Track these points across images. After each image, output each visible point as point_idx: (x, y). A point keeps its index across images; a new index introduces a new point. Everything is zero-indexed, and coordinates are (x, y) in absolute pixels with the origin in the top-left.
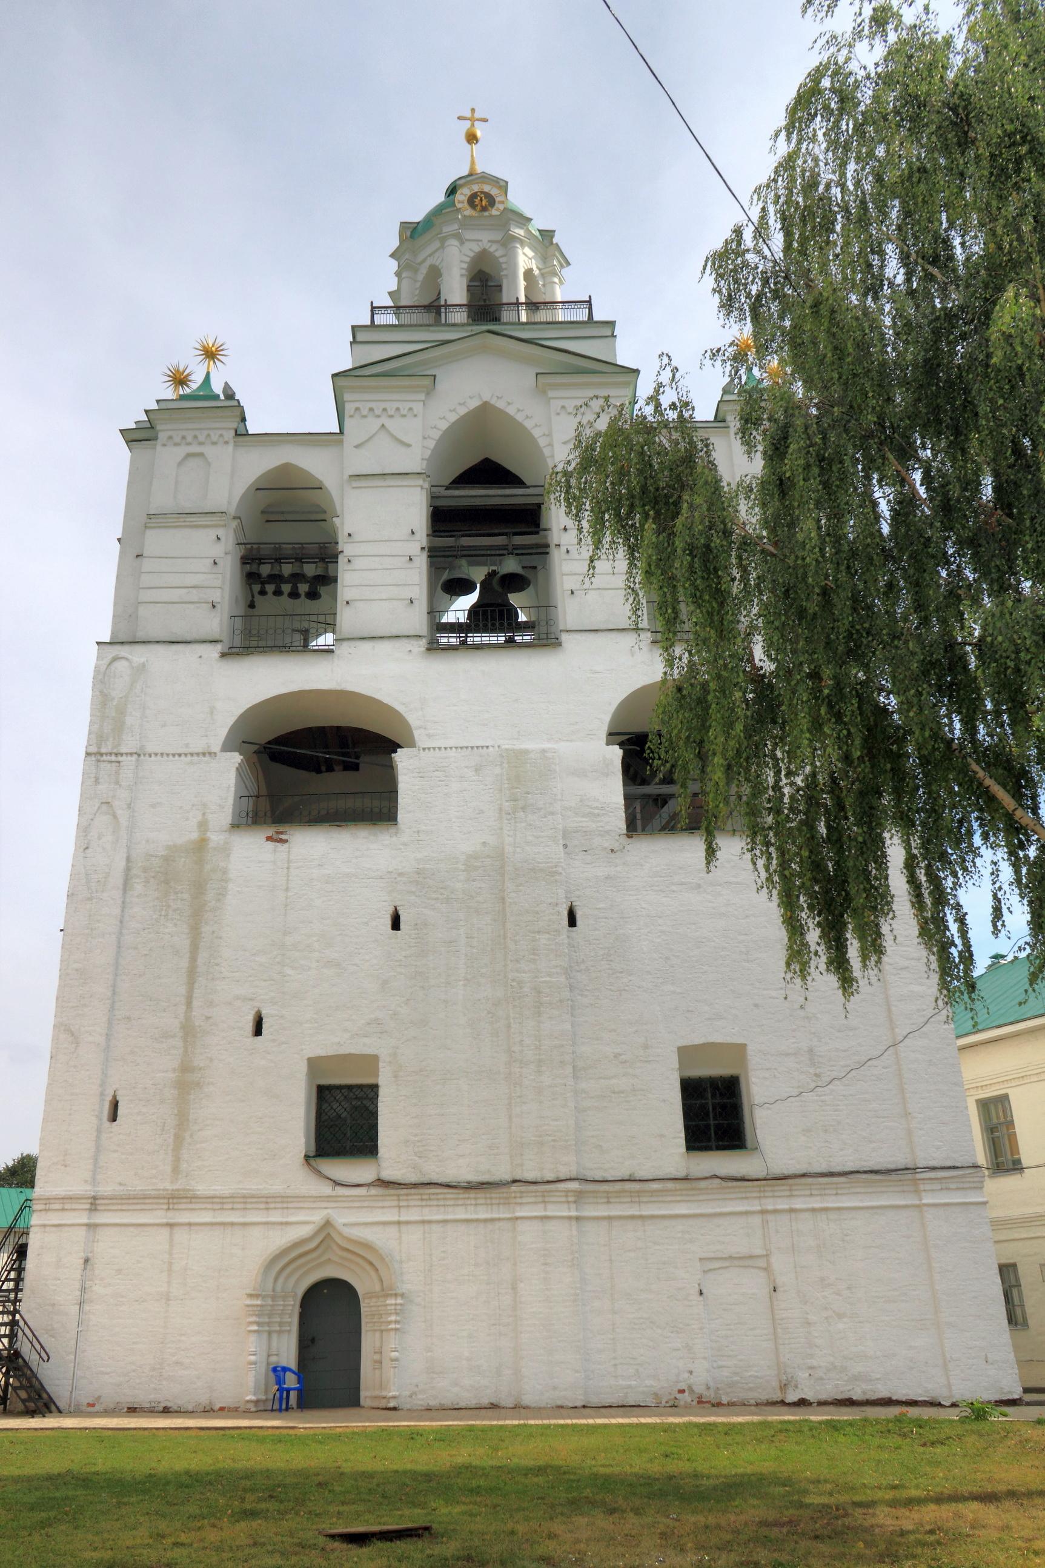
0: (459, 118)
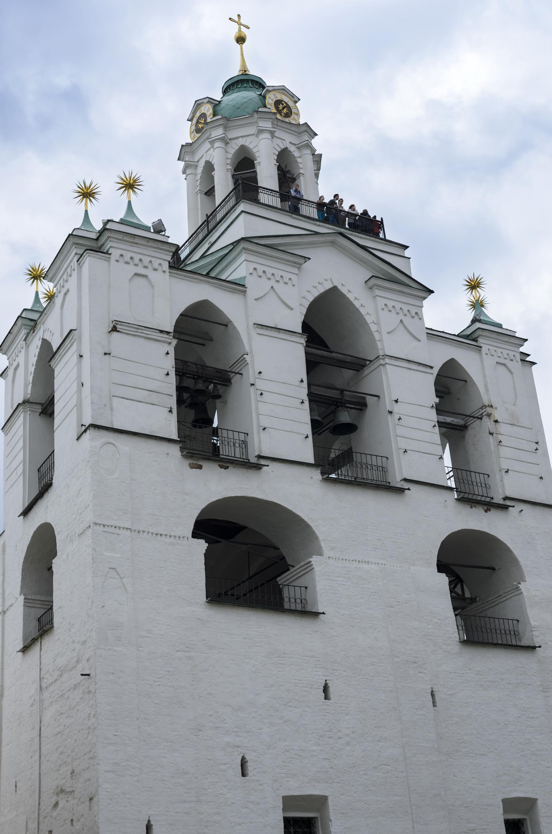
0: (230, 19)
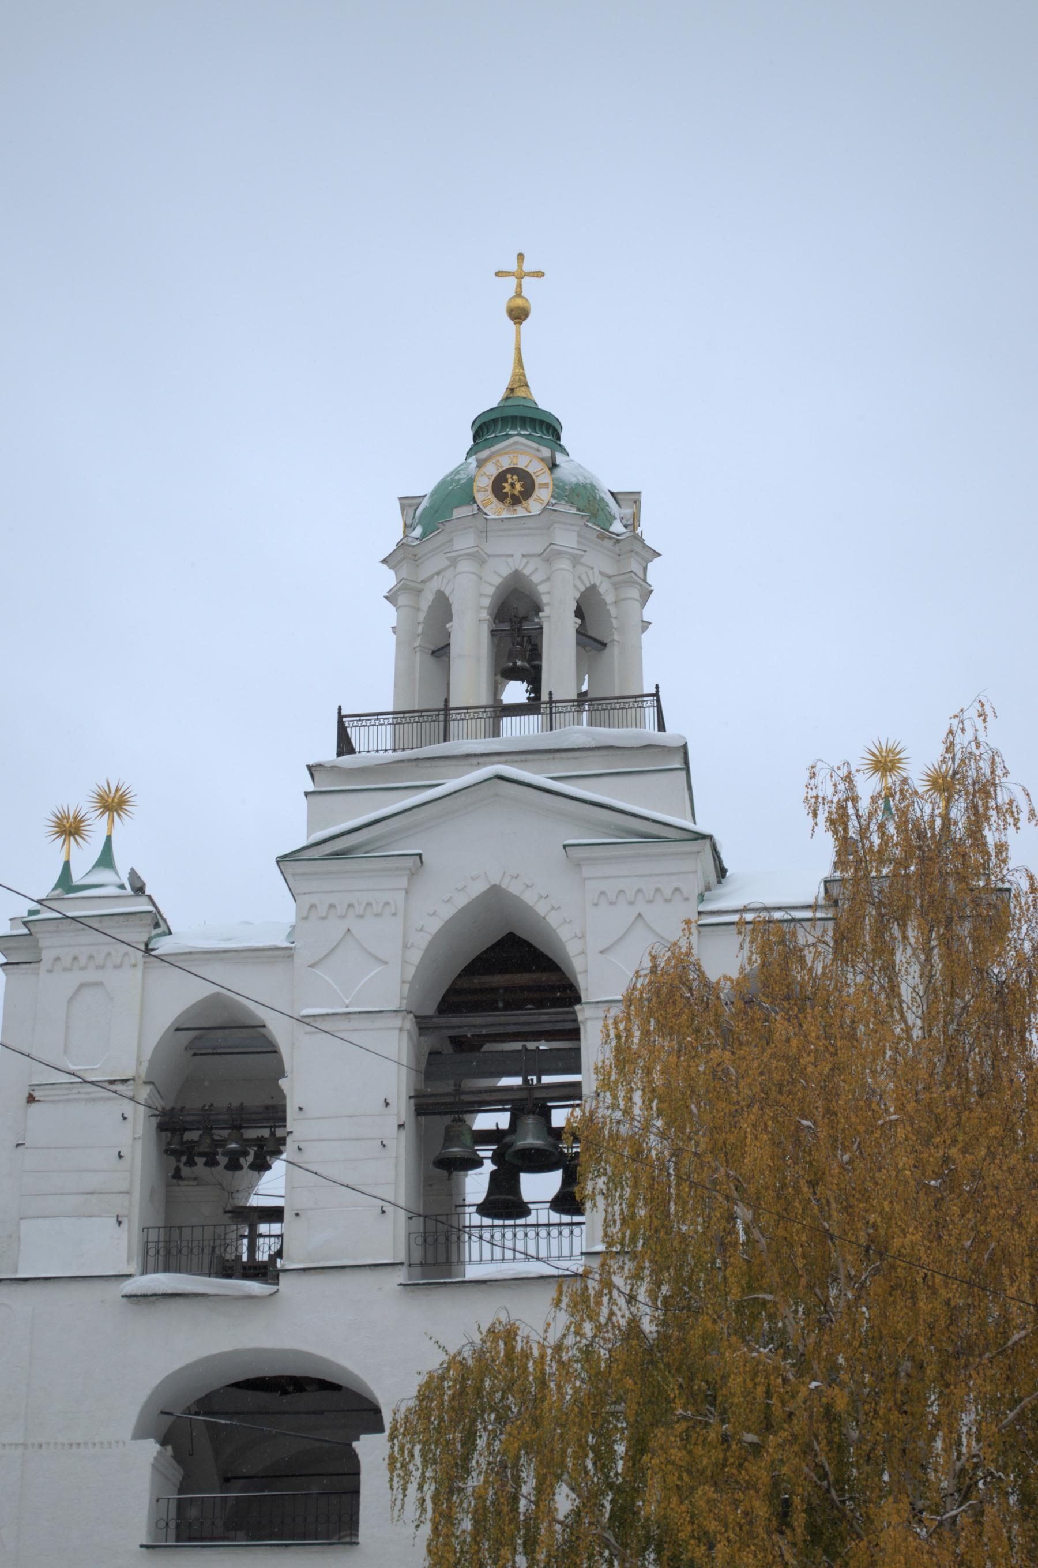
0: (497, 274)
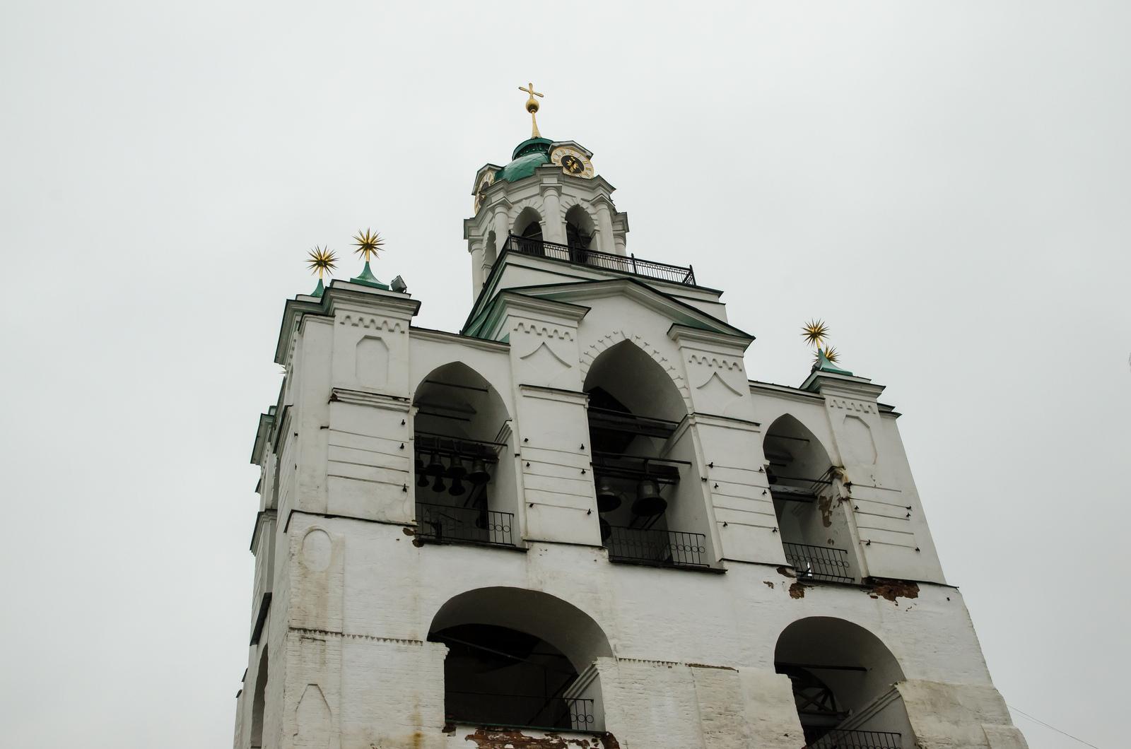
0: (520, 88)
